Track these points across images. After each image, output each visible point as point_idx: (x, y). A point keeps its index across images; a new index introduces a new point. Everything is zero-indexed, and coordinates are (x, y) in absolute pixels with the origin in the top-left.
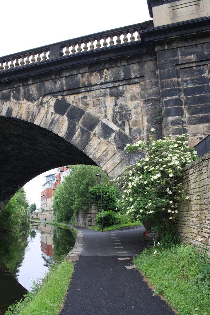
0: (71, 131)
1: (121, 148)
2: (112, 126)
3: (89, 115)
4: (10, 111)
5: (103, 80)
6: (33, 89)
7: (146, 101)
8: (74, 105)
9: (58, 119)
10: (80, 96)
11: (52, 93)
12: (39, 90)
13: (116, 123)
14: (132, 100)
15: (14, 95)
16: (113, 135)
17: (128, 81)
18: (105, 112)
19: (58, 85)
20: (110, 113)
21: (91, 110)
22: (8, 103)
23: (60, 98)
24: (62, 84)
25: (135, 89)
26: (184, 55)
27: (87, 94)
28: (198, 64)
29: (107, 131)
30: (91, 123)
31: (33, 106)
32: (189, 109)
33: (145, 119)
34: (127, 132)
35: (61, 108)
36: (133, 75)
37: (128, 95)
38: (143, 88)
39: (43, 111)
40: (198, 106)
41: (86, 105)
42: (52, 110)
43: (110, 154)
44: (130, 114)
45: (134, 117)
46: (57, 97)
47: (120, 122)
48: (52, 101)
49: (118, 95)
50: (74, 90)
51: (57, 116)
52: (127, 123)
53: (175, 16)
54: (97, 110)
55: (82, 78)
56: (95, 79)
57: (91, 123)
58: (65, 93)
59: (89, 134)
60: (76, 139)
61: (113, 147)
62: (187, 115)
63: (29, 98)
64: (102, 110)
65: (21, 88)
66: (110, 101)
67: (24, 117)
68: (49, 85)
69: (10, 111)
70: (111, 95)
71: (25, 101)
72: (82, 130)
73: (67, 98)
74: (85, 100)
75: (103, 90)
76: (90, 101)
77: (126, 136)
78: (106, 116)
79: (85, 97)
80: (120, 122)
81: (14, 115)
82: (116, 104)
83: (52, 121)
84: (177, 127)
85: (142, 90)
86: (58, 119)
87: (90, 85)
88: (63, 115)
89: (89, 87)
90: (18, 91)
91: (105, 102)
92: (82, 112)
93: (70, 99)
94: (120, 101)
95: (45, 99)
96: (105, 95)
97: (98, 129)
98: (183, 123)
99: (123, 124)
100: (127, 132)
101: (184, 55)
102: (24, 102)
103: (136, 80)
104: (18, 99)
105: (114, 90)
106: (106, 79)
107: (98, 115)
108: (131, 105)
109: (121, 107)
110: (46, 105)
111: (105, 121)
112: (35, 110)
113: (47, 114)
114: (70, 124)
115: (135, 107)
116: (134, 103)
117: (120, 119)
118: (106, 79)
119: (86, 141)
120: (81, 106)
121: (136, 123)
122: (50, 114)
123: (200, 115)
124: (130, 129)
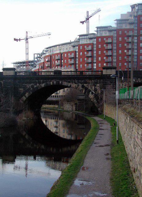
4: (70, 85)
6: (76, 81)
11: (81, 83)
12: (78, 82)
17: (97, 83)
20: (93, 89)
21: (89, 88)
25: (98, 85)
30: (90, 91)
35: (83, 87)
50: (86, 83)
55: (87, 81)
57: (90, 91)
63: (75, 83)
79: (88, 85)
92: (88, 88)
93: (85, 85)
97: (90, 93)
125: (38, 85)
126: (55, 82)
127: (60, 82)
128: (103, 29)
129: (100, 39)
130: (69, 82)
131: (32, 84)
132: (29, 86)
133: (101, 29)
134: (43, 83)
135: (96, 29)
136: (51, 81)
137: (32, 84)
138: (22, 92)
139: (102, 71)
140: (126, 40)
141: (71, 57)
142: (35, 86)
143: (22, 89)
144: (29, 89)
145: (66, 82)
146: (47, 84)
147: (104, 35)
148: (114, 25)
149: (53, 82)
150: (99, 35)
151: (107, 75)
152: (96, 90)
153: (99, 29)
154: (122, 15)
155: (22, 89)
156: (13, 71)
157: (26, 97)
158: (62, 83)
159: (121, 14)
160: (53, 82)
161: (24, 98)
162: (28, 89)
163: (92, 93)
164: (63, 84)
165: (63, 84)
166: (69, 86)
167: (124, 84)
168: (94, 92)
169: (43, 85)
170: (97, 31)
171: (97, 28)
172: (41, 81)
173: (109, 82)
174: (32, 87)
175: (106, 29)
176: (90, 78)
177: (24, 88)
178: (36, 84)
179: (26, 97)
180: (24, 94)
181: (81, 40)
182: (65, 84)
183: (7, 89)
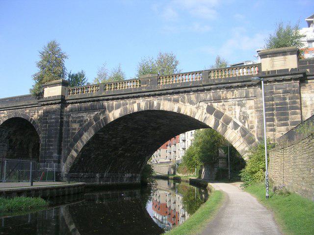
0: (216, 124)
1: (243, 136)
3: (226, 116)
4: (179, 109)
5: (234, 97)
7: (257, 111)
8: (218, 109)
9: (209, 117)
10: (221, 104)
11: (204, 101)
12: (197, 98)
13: (241, 121)
14: (250, 109)
15: (181, 99)
17: (247, 97)
18: (235, 114)
20: (238, 116)
21: (227, 113)
23: (209, 104)
24: (210, 96)
25: (251, 103)
26: (276, 89)
28: (284, 94)
29: (236, 126)
31: (193, 107)
32: (278, 118)
33: (256, 121)
34: (247, 127)
35: (210, 110)
36: (250, 95)
37: (248, 106)
39: (200, 112)
40: (282, 117)
41: (225, 109)
42: (205, 111)
43: (238, 138)
45: (250, 119)
47: (243, 121)
48: (204, 105)
49: (241, 105)
50: (218, 100)
52: (246, 122)
53: (273, 66)
54: (231, 113)
55: (222, 93)
56: (229, 95)
57: (227, 121)
58: (212, 101)
60: (220, 129)
61: (239, 134)
62: (276, 121)
63: (191, 103)
64: (234, 113)
65: (186, 96)
66: (238, 109)
67: (188, 114)
68: (202, 95)
69: (179, 109)
70: (238, 105)
71: (189, 104)
72: (222, 124)
73: (213, 104)
74: (223, 106)
75: (234, 102)
76: (227, 107)
77: (246, 129)
78: (235, 117)
79: (224, 105)
80: (243, 121)
81: (182, 112)
82: (241, 111)
83: (206, 117)
84: (271, 128)
85: (255, 104)
86: (209, 117)
87: (226, 99)
89: (226, 99)
90: (184, 98)
93: (215, 105)
94: (243, 109)
95: (201, 104)
97: (231, 125)
98: (274, 125)
99: (245, 122)
100: (247, 127)
101: (277, 89)
103: (252, 98)
105: (240, 102)
106: (236, 96)
108: (249, 112)
109: (244, 113)
110: (202, 108)
111: (235, 120)
112: (195, 110)
114: (215, 121)
116: (251, 111)
117: (243, 119)
118: (236, 96)
119: (225, 130)
120: (222, 110)
121: (251, 122)
122: (204, 114)
123: (282, 122)
124: (248, 125)
130: (176, 101)
131: (96, 113)
134: (118, 107)
136: (135, 102)
138: (77, 131)
139: (259, 66)
142: (102, 117)
143: (76, 126)
144: (90, 124)
145: (170, 100)
146: (126, 109)
149: (139, 105)
152: (245, 118)
155: (76, 126)
157: (82, 142)
158: (159, 105)
160: (139, 105)
161: (80, 145)
162: (89, 123)
163: (236, 126)
165: (161, 108)
173: (281, 91)
174: (96, 118)
177: (81, 122)
179: (82, 142)
180: (80, 134)
182: (166, 105)
183: (49, 126)
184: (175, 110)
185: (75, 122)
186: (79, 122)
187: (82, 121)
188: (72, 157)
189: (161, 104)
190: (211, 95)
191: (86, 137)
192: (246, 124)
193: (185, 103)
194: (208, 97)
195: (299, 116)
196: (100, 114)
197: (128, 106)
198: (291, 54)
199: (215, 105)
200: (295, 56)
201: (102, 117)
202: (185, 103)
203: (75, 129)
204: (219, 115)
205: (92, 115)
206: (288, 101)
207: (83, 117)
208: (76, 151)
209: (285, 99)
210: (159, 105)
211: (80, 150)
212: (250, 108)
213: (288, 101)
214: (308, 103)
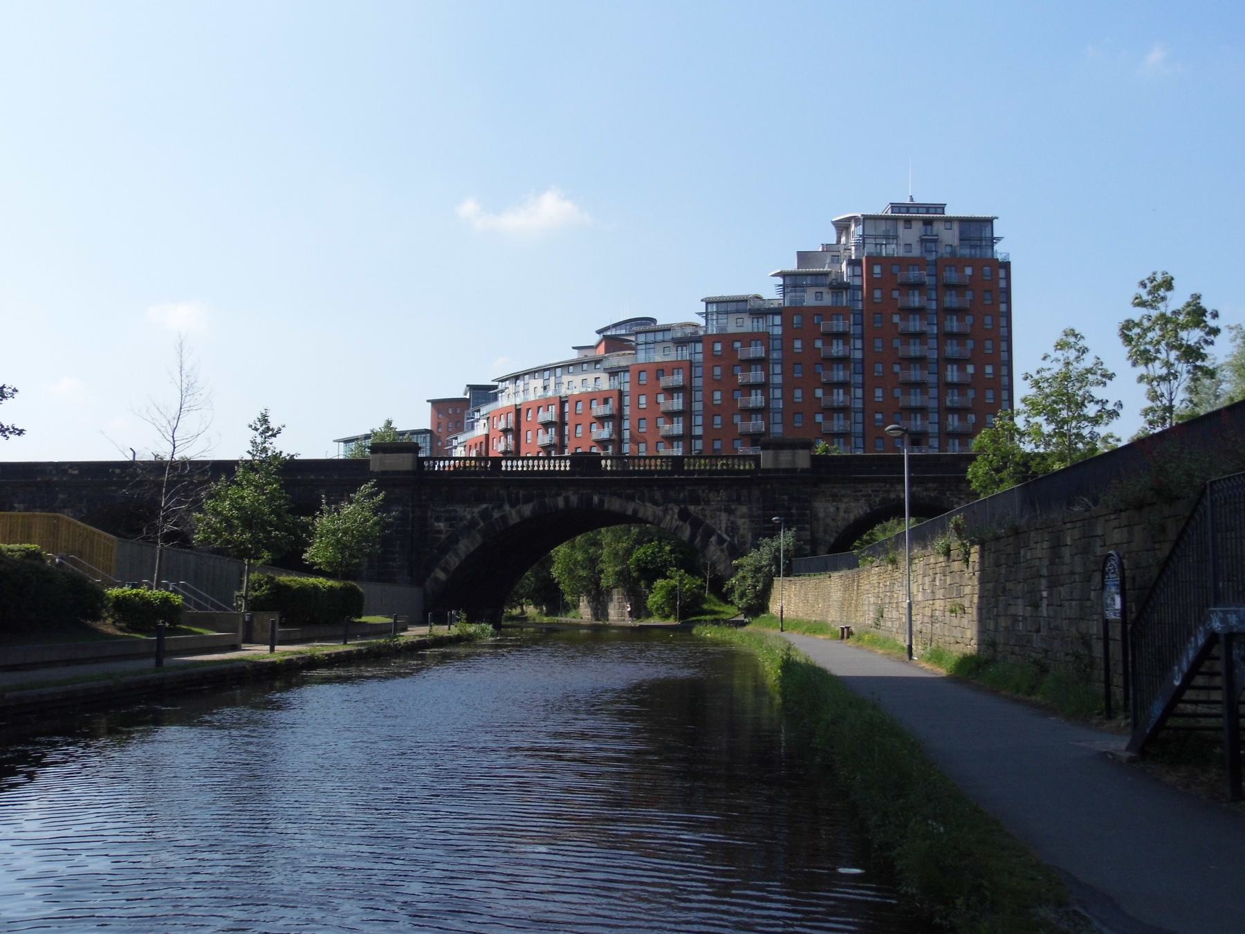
2: (725, 536)
4: (635, 512)
5: (719, 498)
6: (658, 495)
7: (753, 521)
8: (695, 514)
10: (700, 507)
11: (677, 502)
13: (728, 535)
16: (725, 545)
17: (739, 501)
18: (720, 524)
19: (682, 495)
20: (723, 529)
21: (709, 521)
22: (633, 504)
23: (682, 506)
25: (743, 509)
27: (705, 507)
29: (721, 541)
30: (709, 532)
31: (659, 510)
33: (750, 534)
35: (684, 515)
36: (743, 499)
37: (738, 513)
38: (750, 509)
39: (668, 517)
41: (705, 516)
42: (676, 516)
44: (739, 529)
45: (742, 531)
46: (679, 506)
49: (730, 511)
50: (696, 501)
51: (681, 523)
57: (709, 532)
59: (708, 541)
63: (655, 503)
64: (718, 522)
66: (724, 516)
69: (635, 512)
76: (708, 513)
78: (720, 529)
79: (703, 509)
81: (640, 515)
86: (682, 526)
88: (686, 522)
89: (708, 502)
91: (720, 516)
93: (692, 508)
94: (732, 518)
95: (671, 505)
96: (720, 511)
97: (713, 539)
99: (733, 536)
100: (736, 542)
102: (649, 505)
104: (642, 499)
107: (714, 527)
108: (740, 522)
109: (733, 523)
110: (670, 512)
111: (719, 532)
112: (661, 514)
113: (672, 518)
114: (691, 531)
115: (744, 524)
116: (743, 520)
120: (701, 517)
121: (743, 536)
122: (674, 521)
124: (738, 540)
125: (507, 507)
126: (574, 499)
127: (596, 499)
128: (732, 307)
129: (718, 347)
130: (631, 498)
131: (484, 506)
132: (468, 513)
133: (723, 307)
134: (527, 500)
135: (702, 308)
136: (559, 495)
137: (484, 506)
138: (443, 536)
140: (896, 324)
141: (745, 357)
142: (496, 515)
144: (473, 524)
145: (620, 496)
147: (732, 328)
148: (770, 291)
149: (567, 499)
150: (713, 330)
151: (777, 470)
152: (733, 529)
153: (714, 308)
154: (803, 257)
156: (411, 455)
158: (602, 502)
159: (799, 253)
160: (567, 499)
161: (453, 561)
163: (721, 541)
164: (606, 506)
166: (630, 512)
167: (843, 506)
168: (728, 539)
169: (527, 510)
170: (706, 315)
171: (708, 302)
172: (521, 492)
173: (785, 497)
174: (485, 515)
175: (741, 306)
176: (713, 481)
177: (452, 519)
178: (500, 507)
180: (453, 540)
181: (643, 347)
182: (614, 504)
184: (630, 512)
185: (438, 519)
186: (446, 520)
187: (454, 518)
188: (436, 580)
189: (606, 501)
190: (686, 493)
191: (465, 547)
192: (736, 539)
193: (644, 502)
194: (682, 495)
195: (808, 533)
196: (493, 509)
197: (547, 500)
198: (803, 448)
199: (692, 508)
200: (806, 451)
201: (496, 515)
202: (644, 502)
203: (440, 532)
204: (696, 524)
205: (476, 510)
206: (794, 511)
207: (455, 511)
208: (445, 570)
209: (790, 508)
210: (602, 502)
211: (452, 568)
212: (742, 517)
213: (794, 511)
214: (821, 515)
